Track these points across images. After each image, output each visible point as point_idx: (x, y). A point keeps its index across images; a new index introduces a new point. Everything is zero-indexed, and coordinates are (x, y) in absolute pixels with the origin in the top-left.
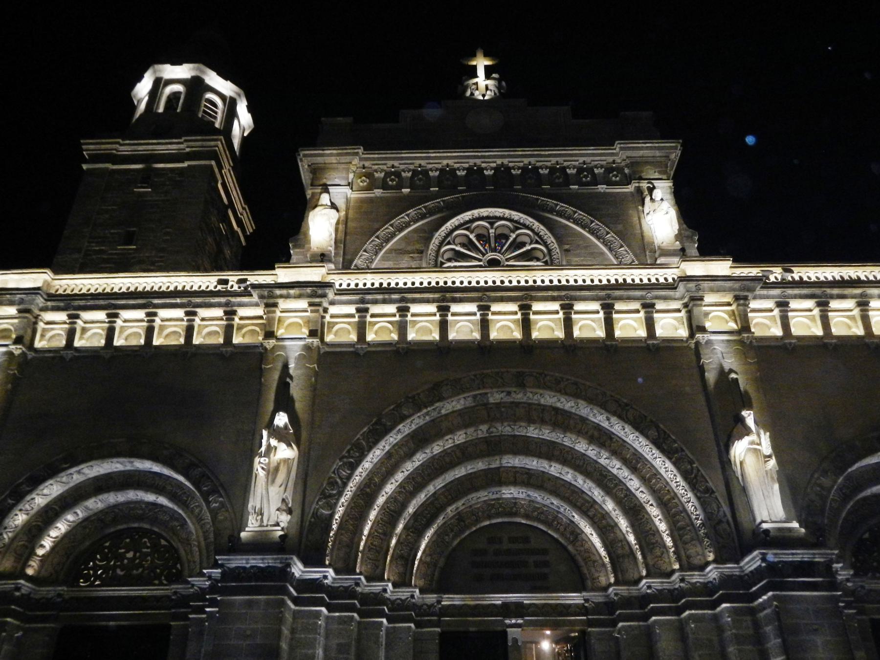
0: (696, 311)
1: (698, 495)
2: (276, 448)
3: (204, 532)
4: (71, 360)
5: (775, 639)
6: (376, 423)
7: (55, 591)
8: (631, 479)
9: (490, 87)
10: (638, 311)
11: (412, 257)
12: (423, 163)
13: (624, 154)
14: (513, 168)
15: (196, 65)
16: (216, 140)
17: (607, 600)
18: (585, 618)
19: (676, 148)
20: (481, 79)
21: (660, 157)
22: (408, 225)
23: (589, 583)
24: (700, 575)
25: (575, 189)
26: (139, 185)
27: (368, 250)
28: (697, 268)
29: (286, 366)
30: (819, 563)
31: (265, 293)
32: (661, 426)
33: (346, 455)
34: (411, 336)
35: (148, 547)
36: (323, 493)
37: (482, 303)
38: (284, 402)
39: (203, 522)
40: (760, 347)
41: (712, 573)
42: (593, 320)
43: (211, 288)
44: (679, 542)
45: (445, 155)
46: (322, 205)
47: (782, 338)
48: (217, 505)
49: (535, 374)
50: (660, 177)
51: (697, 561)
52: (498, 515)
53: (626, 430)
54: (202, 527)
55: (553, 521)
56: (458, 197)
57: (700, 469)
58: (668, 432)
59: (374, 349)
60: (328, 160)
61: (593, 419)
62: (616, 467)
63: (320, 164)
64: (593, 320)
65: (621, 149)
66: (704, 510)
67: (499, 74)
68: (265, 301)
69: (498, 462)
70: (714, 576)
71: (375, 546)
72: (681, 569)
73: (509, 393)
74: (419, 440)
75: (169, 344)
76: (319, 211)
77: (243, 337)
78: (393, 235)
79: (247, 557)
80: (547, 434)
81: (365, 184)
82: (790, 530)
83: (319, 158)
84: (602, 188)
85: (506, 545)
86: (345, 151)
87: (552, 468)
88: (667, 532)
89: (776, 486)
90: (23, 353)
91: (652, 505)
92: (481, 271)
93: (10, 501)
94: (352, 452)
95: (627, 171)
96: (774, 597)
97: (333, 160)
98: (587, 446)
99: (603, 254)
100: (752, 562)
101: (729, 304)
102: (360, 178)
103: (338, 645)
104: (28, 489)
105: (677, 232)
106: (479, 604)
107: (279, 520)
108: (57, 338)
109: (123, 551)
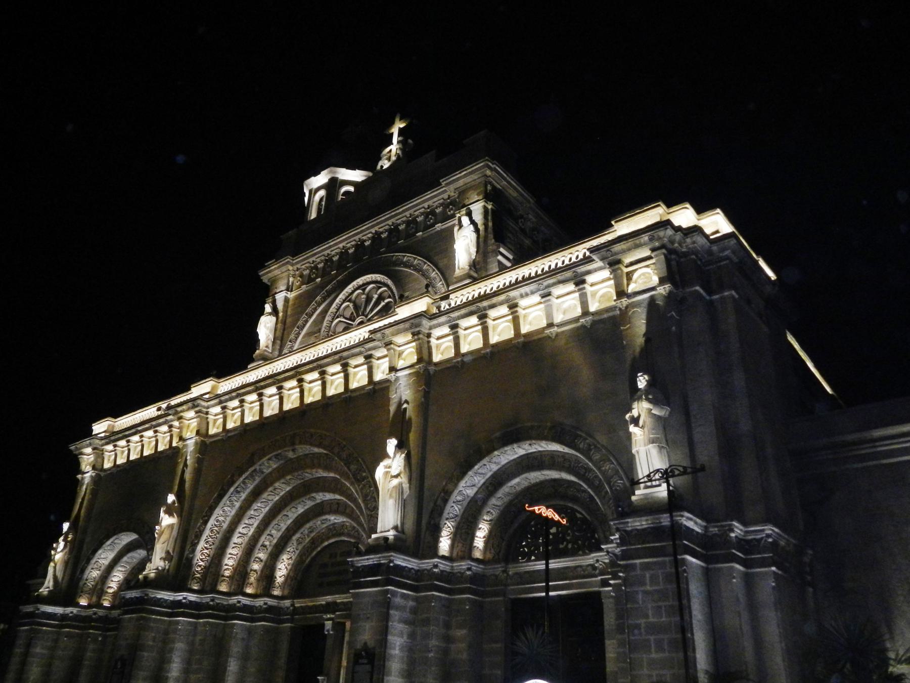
11: (316, 336)
15: (329, 169)
21: (479, 178)
22: (315, 309)
25: (419, 236)
29: (186, 460)
45: (339, 240)
60: (277, 272)
63: (273, 277)
65: (447, 184)
74: (255, 495)
81: (299, 282)
83: (269, 274)
86: (281, 263)
97: (277, 272)
103: (200, 640)
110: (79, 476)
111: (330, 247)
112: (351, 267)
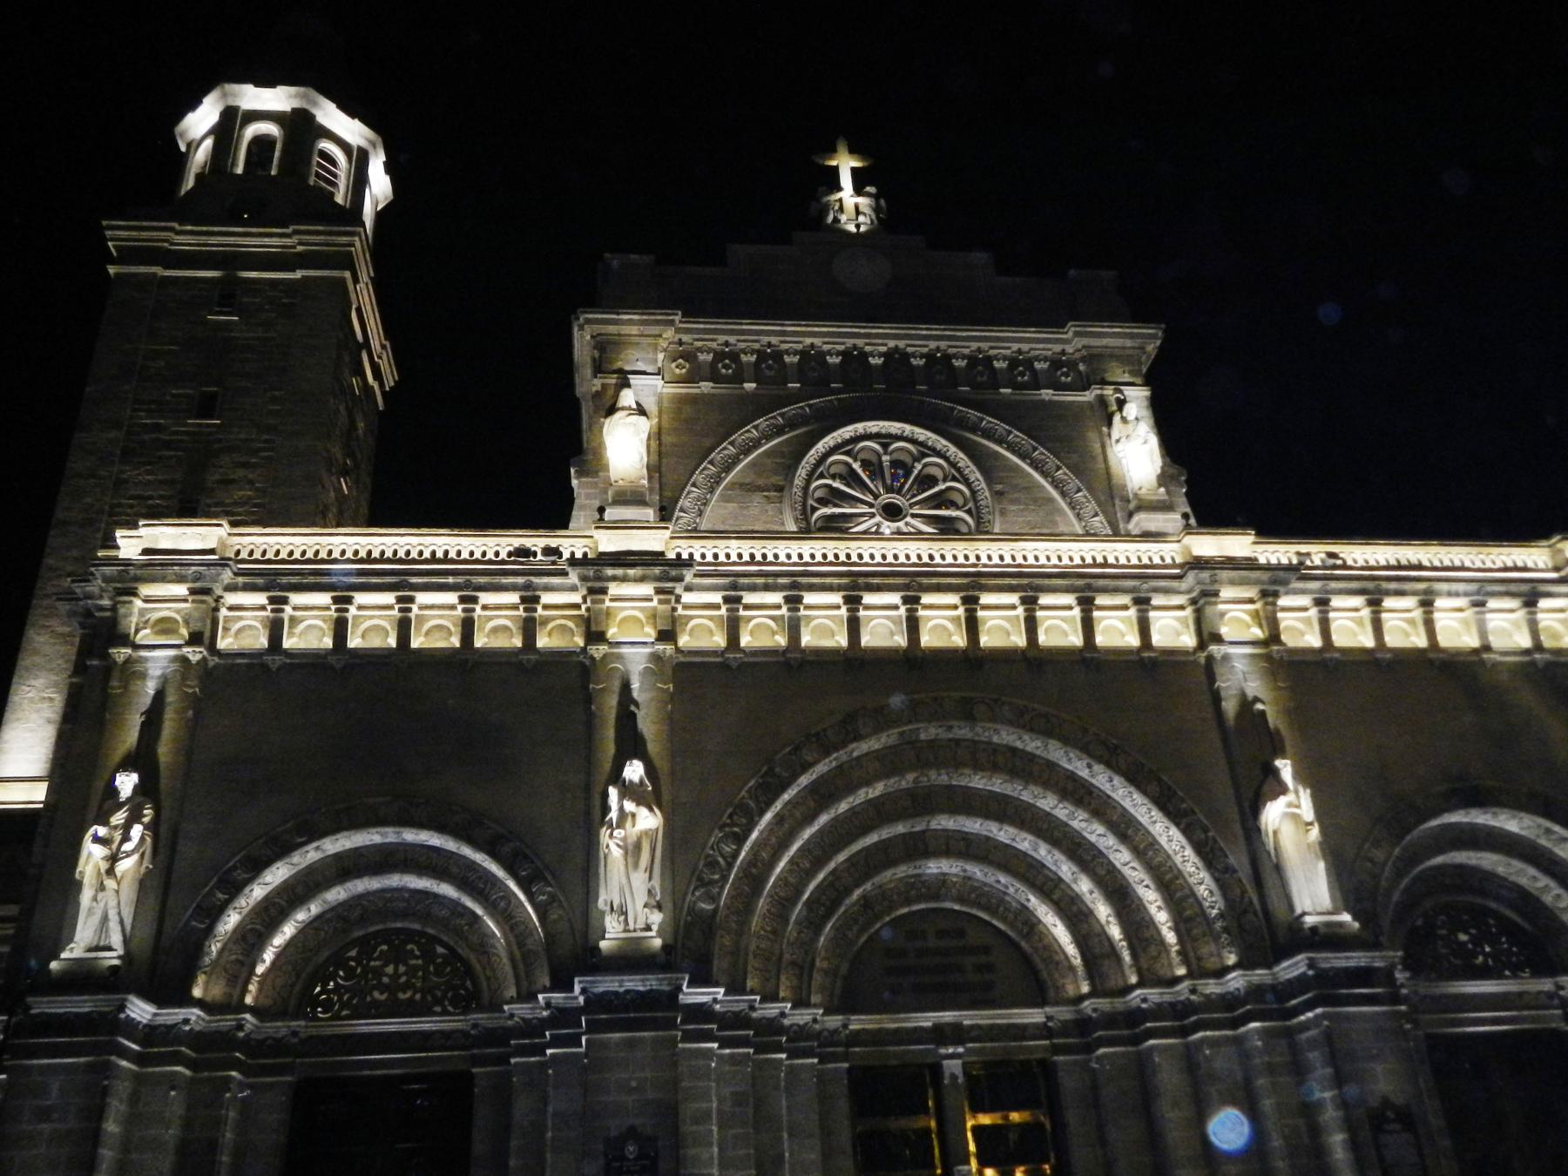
0: (1209, 610)
1: (1216, 875)
2: (633, 815)
3: (516, 937)
5: (1323, 1067)
6: (766, 773)
7: (289, 1027)
8: (1117, 850)
9: (861, 209)
10: (1125, 608)
11: (766, 497)
12: (774, 340)
13: (1080, 342)
14: (913, 355)
15: (302, 89)
16: (352, 234)
17: (1079, 1017)
18: (1047, 1042)
19: (1153, 337)
20: (847, 193)
21: (1133, 348)
22: (757, 444)
23: (1051, 994)
24: (1216, 984)
25: (1005, 394)
26: (217, 309)
27: (698, 484)
28: (1209, 545)
29: (626, 687)
30: (1378, 969)
32: (1165, 778)
33: (728, 821)
34: (806, 640)
35: (417, 958)
36: (700, 879)
37: (909, 593)
38: (631, 745)
39: (513, 921)
40: (1291, 663)
41: (1236, 981)
42: (1063, 619)
44: (1186, 938)
46: (623, 409)
47: (1320, 651)
48: (544, 898)
49: (987, 701)
50: (1131, 380)
51: (1213, 963)
52: (919, 899)
53: (1115, 782)
54: (512, 929)
55: (998, 907)
56: (830, 401)
57: (1219, 840)
58: (1174, 787)
59: (751, 659)
60: (626, 330)
61: (1067, 766)
62: (1096, 833)
63: (611, 335)
64: (1063, 619)
65: (1077, 334)
66: (1225, 895)
67: (877, 188)
68: (589, 584)
69: (924, 824)
70: (1237, 986)
71: (762, 949)
72: (1190, 975)
73: (950, 728)
74: (822, 795)
76: (620, 418)
77: (550, 634)
78: (735, 460)
79: (622, 978)
80: (998, 785)
81: (684, 370)
82: (1341, 924)
84: (1047, 394)
85: (932, 942)
87: (1002, 833)
88: (1169, 924)
89: (1322, 865)
90: (204, 658)
91: (1147, 886)
93: (220, 896)
94: (735, 818)
95: (1082, 367)
96: (1324, 1016)
97: (634, 330)
98: (1056, 802)
99: (1051, 500)
100: (1292, 967)
101: (1251, 601)
102: (674, 360)
103: (732, 1093)
104: (246, 876)
105: (1159, 471)
106: (902, 1028)
107: (649, 921)
109: (378, 963)
110: (121, 653)
111: (783, 333)
112: (839, 391)
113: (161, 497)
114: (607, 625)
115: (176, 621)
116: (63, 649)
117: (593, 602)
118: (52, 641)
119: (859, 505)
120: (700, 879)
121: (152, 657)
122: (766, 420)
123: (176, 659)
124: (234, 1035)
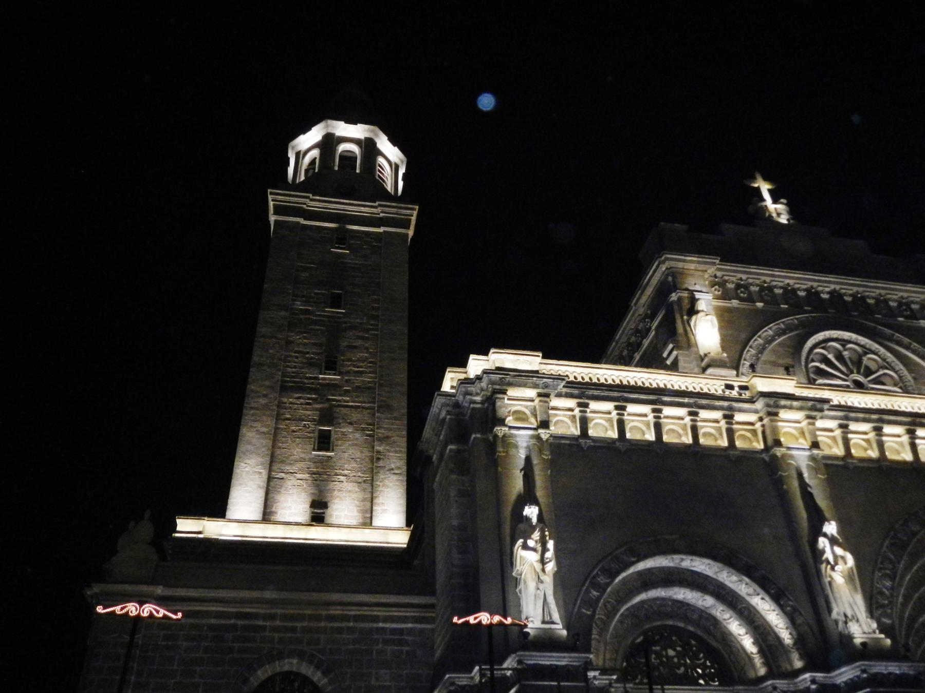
4: (589, 447)
9: (779, 211)
12: (768, 279)
29: (800, 475)
31: (771, 401)
43: (720, 392)
45: (788, 274)
60: (687, 266)
68: (770, 410)
75: (671, 441)
81: (720, 293)
92: (920, 398)
97: (692, 266)
102: (712, 287)
108: (561, 424)
111: (773, 276)
113: (313, 353)
114: (779, 436)
115: (525, 413)
116: (264, 442)
117: (772, 421)
118: (258, 436)
119: (838, 380)
120: (877, 602)
121: (519, 435)
122: (775, 325)
123: (532, 437)
124: (608, 690)
